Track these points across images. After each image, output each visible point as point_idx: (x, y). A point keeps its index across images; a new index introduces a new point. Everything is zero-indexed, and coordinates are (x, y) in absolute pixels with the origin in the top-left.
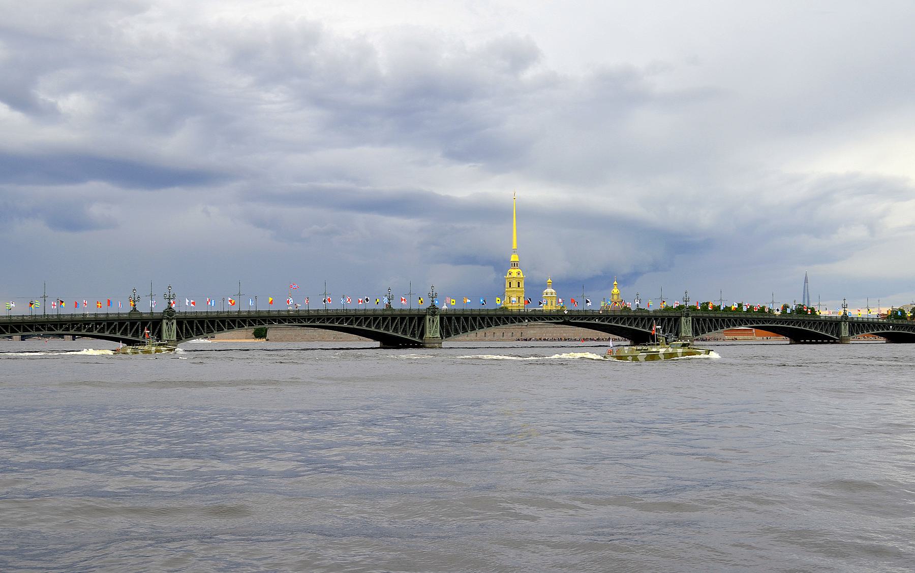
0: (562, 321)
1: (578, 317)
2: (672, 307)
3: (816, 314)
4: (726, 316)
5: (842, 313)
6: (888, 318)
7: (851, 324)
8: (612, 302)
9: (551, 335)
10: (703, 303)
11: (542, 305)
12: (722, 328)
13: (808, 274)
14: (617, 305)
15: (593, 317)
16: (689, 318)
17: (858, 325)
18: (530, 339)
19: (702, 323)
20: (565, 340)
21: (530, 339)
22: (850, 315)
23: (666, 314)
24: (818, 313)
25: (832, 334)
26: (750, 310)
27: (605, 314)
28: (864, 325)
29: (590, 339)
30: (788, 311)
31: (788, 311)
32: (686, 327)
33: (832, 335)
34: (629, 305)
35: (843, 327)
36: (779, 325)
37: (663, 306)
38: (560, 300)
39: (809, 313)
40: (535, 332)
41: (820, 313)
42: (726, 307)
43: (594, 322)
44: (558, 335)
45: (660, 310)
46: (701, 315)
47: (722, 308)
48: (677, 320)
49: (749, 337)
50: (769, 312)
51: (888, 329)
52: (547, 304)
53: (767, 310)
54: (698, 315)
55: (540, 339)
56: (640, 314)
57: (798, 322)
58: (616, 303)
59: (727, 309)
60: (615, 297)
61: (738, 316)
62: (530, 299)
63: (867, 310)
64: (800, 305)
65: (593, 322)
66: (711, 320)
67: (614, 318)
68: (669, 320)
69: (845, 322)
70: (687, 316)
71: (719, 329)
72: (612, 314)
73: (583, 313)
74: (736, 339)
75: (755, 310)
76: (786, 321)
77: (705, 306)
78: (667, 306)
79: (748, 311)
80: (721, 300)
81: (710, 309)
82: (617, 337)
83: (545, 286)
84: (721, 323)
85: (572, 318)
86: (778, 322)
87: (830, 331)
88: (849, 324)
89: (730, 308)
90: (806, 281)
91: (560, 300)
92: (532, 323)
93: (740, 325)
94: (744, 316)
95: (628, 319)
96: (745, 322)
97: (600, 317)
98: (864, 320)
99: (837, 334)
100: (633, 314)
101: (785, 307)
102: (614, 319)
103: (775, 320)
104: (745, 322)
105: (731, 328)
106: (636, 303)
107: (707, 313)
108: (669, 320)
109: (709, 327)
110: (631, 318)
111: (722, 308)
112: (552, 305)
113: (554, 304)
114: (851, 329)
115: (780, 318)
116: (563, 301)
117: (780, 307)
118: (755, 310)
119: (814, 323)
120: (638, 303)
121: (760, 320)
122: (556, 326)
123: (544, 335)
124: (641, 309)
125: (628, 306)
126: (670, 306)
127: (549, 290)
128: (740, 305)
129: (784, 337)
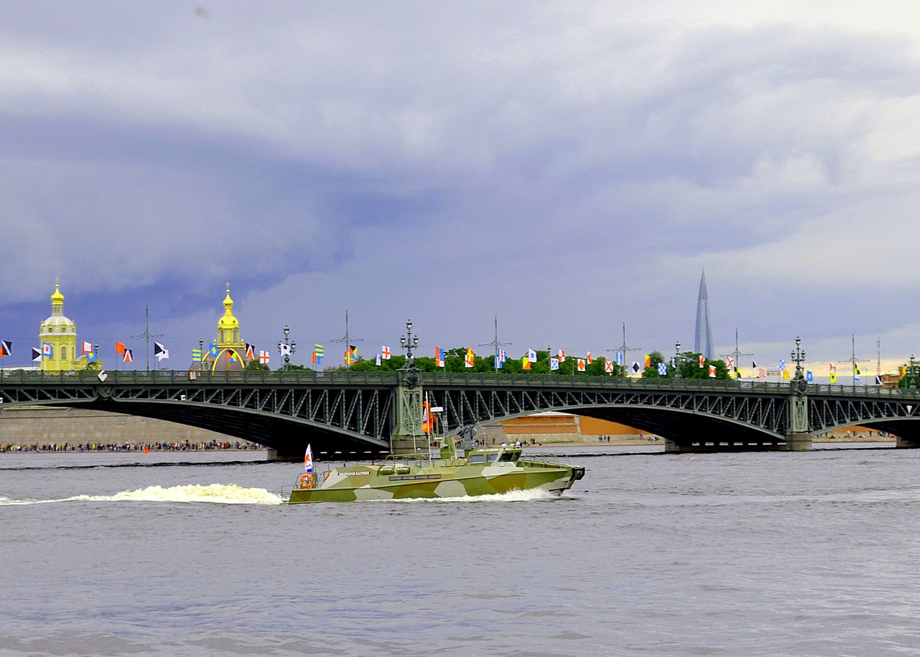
0: (91, 399)
1: (134, 389)
2: (375, 361)
3: (730, 379)
4: (508, 383)
5: (788, 374)
6: (901, 385)
7: (813, 402)
8: (219, 349)
9: (62, 436)
10: (451, 352)
11: (39, 359)
12: (499, 413)
13: (705, 273)
14: (234, 356)
15: (173, 389)
16: (416, 389)
17: (832, 404)
18: (9, 447)
19: (449, 402)
20: (100, 448)
21: (9, 447)
22: (811, 379)
23: (359, 380)
24: (732, 374)
25: (768, 425)
26: (568, 368)
27: (205, 381)
28: (844, 404)
29: (165, 445)
30: (662, 370)
31: (662, 370)
32: (409, 413)
33: (768, 428)
34: (265, 358)
35: (794, 409)
36: (640, 406)
37: (349, 361)
38: (87, 347)
39: (712, 375)
40: (21, 428)
41: (739, 376)
42: (508, 361)
43: (174, 401)
44: (83, 435)
45: (342, 370)
46: (445, 381)
47: (498, 366)
48: (387, 394)
49: (566, 436)
50: (615, 372)
51: (902, 414)
52: (51, 356)
53: (609, 369)
54: (440, 381)
55: (35, 447)
56: (293, 380)
57: (685, 397)
58: (231, 353)
59: (512, 366)
60: (228, 337)
61: (538, 383)
62: (9, 344)
63: (851, 365)
64: (689, 355)
65: (171, 401)
66: (471, 395)
67: (228, 390)
68: (367, 395)
69: (799, 395)
70: (412, 384)
71: (492, 417)
72: (221, 380)
73: (149, 380)
74: (533, 441)
75: (579, 369)
76: (656, 395)
77: (456, 360)
78: (360, 360)
79: (561, 371)
80: (496, 343)
81: (468, 365)
82: (232, 440)
83: (47, 310)
84: (496, 401)
85: (118, 392)
86: (636, 398)
87: (762, 419)
89: (518, 364)
90: (703, 294)
91: (87, 347)
92: (15, 405)
93: (544, 406)
94: (553, 384)
95: (263, 393)
96: (556, 399)
97: (191, 389)
98: (845, 390)
99: (780, 426)
100: (275, 380)
101: (655, 360)
102: (227, 393)
103: (630, 393)
104: (556, 399)
105: (522, 413)
106: (284, 352)
107: (462, 378)
108: (367, 395)
109: (466, 413)
110: (270, 391)
111: (498, 366)
112: (64, 357)
113: (69, 357)
114: (815, 413)
115: (640, 386)
116: (95, 350)
117: (644, 360)
118: (579, 369)
119: (726, 400)
120: (287, 352)
121: (591, 394)
122: (77, 412)
123: (45, 436)
124: (294, 367)
125: (262, 361)
126: (367, 358)
127: (57, 320)
128: (542, 356)
129: (653, 436)
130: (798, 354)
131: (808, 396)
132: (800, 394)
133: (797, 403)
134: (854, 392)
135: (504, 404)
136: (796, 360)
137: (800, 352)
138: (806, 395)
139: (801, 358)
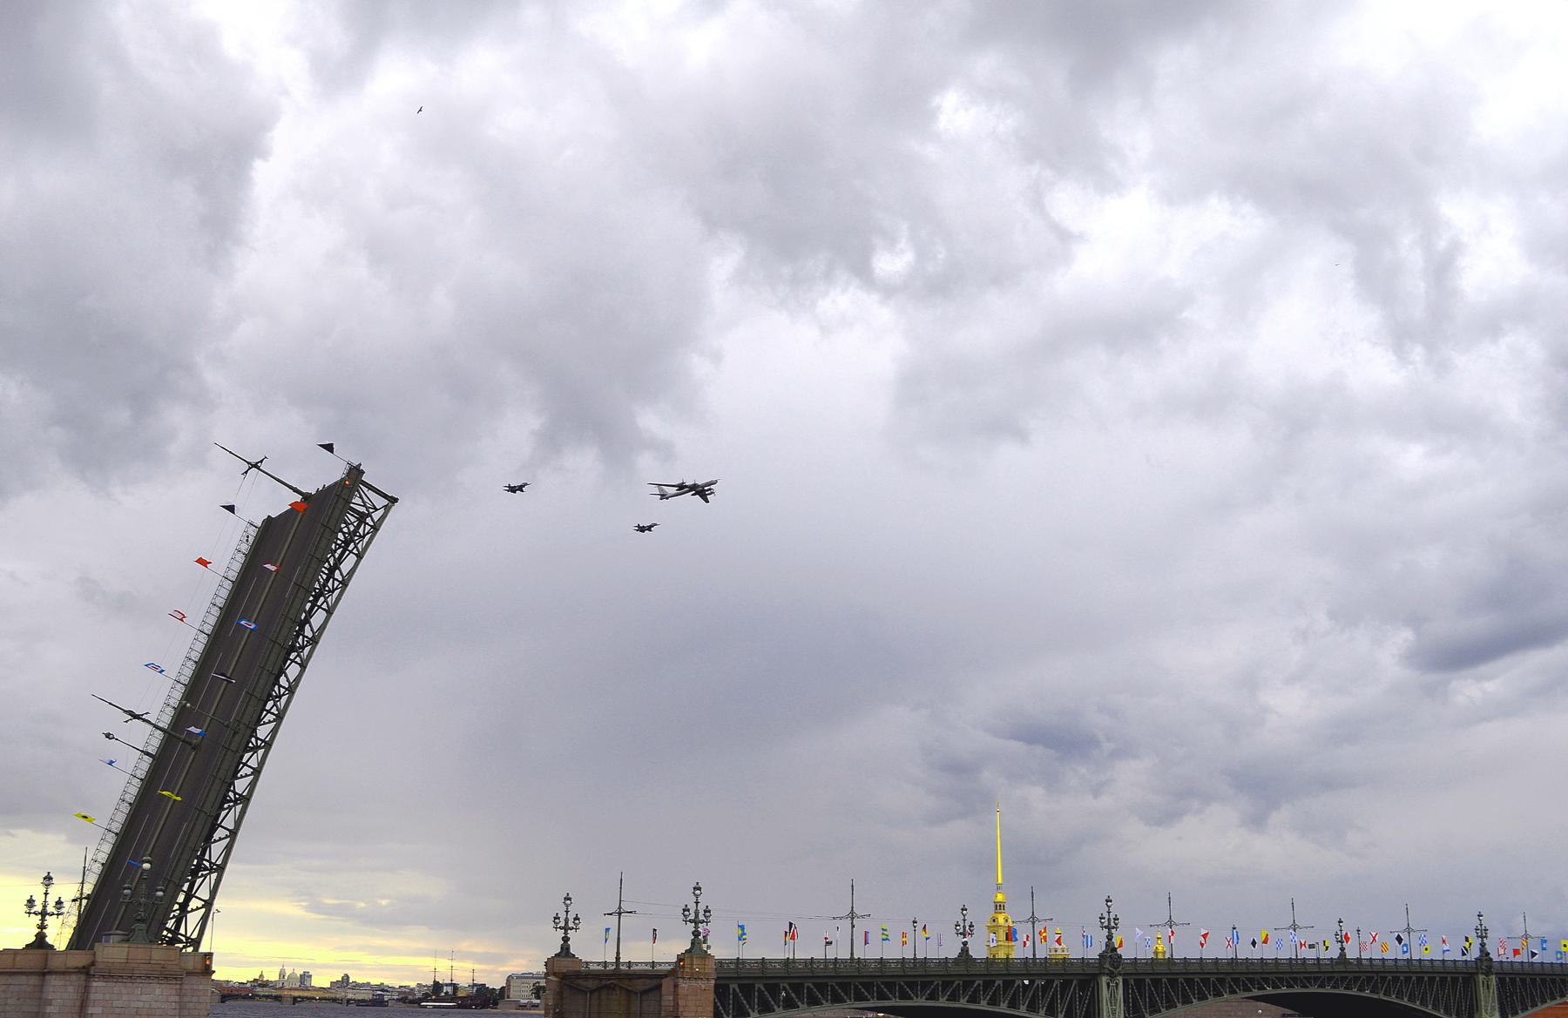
35: (1105, 993)
69: (1112, 975)
88: (1125, 982)
130: (1109, 919)
131: (1125, 974)
132: (1113, 973)
133: (1108, 985)
134: (1455, 967)
135: (1193, 990)
136: (1106, 927)
137: (1112, 916)
138: (1121, 975)
139: (1113, 924)
